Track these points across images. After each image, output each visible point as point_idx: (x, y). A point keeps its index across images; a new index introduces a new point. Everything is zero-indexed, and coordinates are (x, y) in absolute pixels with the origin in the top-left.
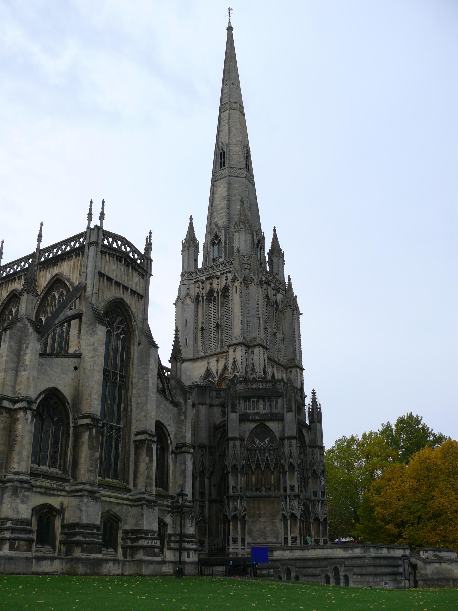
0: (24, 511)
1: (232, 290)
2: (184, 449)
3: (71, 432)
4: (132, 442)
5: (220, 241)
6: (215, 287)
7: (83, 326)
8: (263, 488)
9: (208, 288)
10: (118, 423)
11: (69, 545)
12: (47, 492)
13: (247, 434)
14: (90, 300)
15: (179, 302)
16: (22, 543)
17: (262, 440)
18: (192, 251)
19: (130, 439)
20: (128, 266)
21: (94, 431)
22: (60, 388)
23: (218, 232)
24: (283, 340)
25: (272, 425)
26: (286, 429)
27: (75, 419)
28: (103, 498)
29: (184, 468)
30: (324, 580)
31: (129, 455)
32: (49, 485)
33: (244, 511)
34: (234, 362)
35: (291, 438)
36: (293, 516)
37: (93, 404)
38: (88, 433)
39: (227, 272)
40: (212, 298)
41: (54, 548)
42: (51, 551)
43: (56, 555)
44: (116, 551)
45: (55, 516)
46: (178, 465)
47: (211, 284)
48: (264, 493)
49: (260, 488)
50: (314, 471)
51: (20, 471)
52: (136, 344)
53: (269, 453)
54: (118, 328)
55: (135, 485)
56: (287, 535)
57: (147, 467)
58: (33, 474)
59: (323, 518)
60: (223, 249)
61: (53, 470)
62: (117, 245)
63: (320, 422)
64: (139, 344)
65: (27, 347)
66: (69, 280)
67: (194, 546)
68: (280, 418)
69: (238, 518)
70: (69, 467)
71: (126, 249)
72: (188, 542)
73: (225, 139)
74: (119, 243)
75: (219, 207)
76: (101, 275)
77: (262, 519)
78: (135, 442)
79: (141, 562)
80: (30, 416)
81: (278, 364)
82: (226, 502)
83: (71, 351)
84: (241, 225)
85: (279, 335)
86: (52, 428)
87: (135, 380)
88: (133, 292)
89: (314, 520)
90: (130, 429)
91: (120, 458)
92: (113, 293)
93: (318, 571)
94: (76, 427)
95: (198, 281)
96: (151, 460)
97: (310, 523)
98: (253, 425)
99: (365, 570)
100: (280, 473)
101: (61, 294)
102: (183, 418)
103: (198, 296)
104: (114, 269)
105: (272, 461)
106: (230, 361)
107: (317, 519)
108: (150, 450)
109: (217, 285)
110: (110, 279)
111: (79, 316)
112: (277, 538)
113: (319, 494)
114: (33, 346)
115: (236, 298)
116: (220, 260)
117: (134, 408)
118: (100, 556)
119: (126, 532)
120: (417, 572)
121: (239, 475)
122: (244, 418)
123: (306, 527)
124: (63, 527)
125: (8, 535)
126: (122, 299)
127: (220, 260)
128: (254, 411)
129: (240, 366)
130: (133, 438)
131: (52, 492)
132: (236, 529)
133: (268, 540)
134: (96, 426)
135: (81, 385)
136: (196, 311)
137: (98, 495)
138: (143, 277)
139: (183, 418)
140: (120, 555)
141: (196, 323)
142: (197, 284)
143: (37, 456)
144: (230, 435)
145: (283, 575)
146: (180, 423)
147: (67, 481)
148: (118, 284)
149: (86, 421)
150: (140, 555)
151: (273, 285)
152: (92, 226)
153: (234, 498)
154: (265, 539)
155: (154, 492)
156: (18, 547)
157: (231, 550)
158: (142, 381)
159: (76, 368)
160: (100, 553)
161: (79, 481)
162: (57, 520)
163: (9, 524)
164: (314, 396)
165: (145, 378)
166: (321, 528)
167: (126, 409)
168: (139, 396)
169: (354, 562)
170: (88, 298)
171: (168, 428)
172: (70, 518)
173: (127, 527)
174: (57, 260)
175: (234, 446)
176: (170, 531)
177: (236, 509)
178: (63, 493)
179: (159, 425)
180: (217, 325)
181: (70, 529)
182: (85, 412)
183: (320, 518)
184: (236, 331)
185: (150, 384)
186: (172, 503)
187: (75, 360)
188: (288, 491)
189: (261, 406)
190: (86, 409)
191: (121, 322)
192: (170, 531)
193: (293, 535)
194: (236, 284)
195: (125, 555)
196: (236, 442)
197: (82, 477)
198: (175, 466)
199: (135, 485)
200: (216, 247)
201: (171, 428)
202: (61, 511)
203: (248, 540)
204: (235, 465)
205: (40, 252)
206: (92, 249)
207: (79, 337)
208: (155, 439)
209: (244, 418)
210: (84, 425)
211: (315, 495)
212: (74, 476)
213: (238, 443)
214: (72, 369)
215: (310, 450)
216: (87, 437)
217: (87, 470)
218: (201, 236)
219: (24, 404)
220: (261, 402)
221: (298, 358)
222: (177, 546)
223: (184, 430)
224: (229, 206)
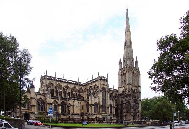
1: (126, 74)
6: (124, 73)
11: (99, 121)
12: (96, 115)
15: (119, 76)
18: (120, 64)
25: (129, 101)
36: (132, 115)
37: (101, 104)
57: (109, 110)
58: (95, 113)
73: (126, 39)
86: (96, 107)
94: (99, 107)
109: (125, 72)
114: (93, 97)
115: (127, 75)
122: (126, 100)
143: (95, 111)
146: (113, 103)
172: (99, 118)
176: (112, 118)
179: (110, 104)
181: (99, 119)
184: (127, 82)
192: (112, 118)
201: (112, 104)
209: (126, 100)
213: (125, 104)
217: (101, 112)
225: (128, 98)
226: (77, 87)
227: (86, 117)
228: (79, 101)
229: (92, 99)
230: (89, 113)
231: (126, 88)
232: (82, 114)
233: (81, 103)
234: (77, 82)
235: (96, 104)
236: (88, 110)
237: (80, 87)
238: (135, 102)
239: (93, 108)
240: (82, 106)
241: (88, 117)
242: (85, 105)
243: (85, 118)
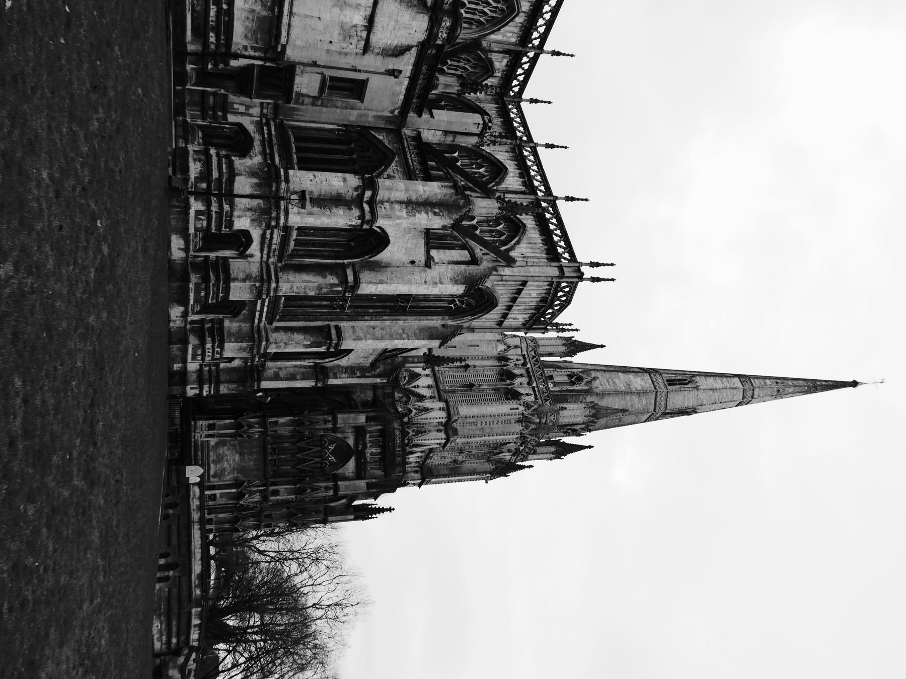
0: (242, 223)
2: (321, 376)
3: (338, 261)
4: (327, 323)
5: (573, 383)
6: (518, 381)
7: (463, 267)
9: (516, 372)
10: (350, 307)
13: (340, 435)
14: (494, 273)
16: (205, 223)
17: (333, 453)
19: (331, 321)
20: (536, 309)
21: (340, 289)
22: (389, 248)
23: (585, 381)
24: (455, 461)
25: (351, 465)
26: (347, 483)
27: (353, 264)
28: (259, 302)
29: (298, 377)
30: (163, 551)
31: (313, 321)
32: (274, 241)
33: (248, 436)
34: (427, 410)
35: (336, 488)
36: (240, 496)
38: (336, 282)
39: (536, 395)
40: (504, 377)
41: (200, 250)
42: (196, 246)
43: (191, 253)
44: (197, 313)
45: (237, 250)
46: (301, 370)
47: (521, 376)
50: (296, 514)
51: (290, 216)
52: (443, 322)
53: (318, 463)
54: (462, 302)
55: (277, 329)
56: (219, 489)
58: (287, 229)
60: (565, 388)
61: (292, 244)
62: (561, 296)
63: (355, 519)
64: (443, 325)
65: (435, 214)
66: (518, 243)
67: (205, 394)
68: (359, 475)
70: (296, 261)
71: (557, 305)
72: (210, 388)
74: (563, 299)
75: (617, 381)
76: (524, 283)
77: (237, 457)
78: (328, 326)
79: (186, 342)
80: (354, 223)
81: (427, 457)
82: (258, 414)
83: (433, 253)
84: (594, 411)
85: (461, 457)
87: (401, 323)
88: (505, 316)
90: (343, 320)
91: (309, 310)
92: (503, 295)
93: (174, 541)
94: (344, 267)
95: (525, 359)
96: (306, 346)
98: (351, 442)
99: (174, 603)
100: (293, 477)
101: (501, 234)
102: (358, 374)
103: (506, 359)
104: (532, 294)
105: (308, 466)
106: (427, 404)
108: (319, 345)
109: (520, 384)
110: (519, 292)
111: (474, 261)
112: (215, 476)
115: (504, 408)
116: (550, 385)
117: (368, 323)
118: (192, 302)
119: (221, 322)
120: (171, 656)
121: (291, 428)
122: (360, 432)
124: (226, 259)
125: (214, 208)
126: (497, 306)
127: (550, 385)
129: (423, 417)
130: (333, 324)
131: (267, 241)
132: (226, 427)
133: (212, 466)
134: (345, 291)
135: (393, 269)
136: (489, 358)
137: (264, 296)
138: (524, 325)
139: (358, 374)
140: (192, 317)
141: (474, 358)
142: (521, 358)
144: (340, 416)
145: (170, 499)
147: (280, 259)
148: (514, 300)
149: (351, 278)
150: (193, 341)
151: (521, 448)
152: (583, 269)
153: (263, 424)
154: (213, 461)
155: (268, 351)
156: (200, 219)
157: (200, 423)
158: (400, 331)
159: (413, 262)
160: (195, 302)
161: (280, 274)
162: (233, 252)
163: (226, 207)
164: (387, 510)
165: (404, 336)
166: (227, 526)
167: (368, 314)
168: (382, 329)
169: (184, 587)
170: (497, 271)
171: (346, 358)
172: (238, 266)
173: (227, 323)
174: (542, 224)
175: (326, 422)
177: (250, 426)
178: (265, 256)
180: (471, 386)
182: (361, 276)
185: (396, 342)
186: (257, 366)
187: (423, 261)
188: (272, 488)
189: (374, 450)
190: (365, 276)
191: (468, 304)
193: (218, 495)
194: (521, 408)
195: (193, 322)
197: (285, 277)
198: (301, 367)
199: (277, 329)
200: (566, 379)
201: (344, 362)
202: (243, 255)
203: (213, 441)
204: (303, 424)
205: (553, 202)
206: (555, 272)
207: (450, 263)
208: (332, 350)
209: (360, 432)
210: (346, 277)
211: (269, 516)
212: (287, 268)
213: (330, 425)
214: (411, 259)
215: (322, 508)
216: (332, 281)
217: (293, 284)
218: (581, 358)
219: (368, 217)
221: (433, 480)
222: (206, 375)
223: (343, 375)
224: (617, 393)
225: (371, 451)
226: (509, 34)
227: (246, 113)
228: (406, 65)
229: (426, 205)
230: (288, 166)
231: (425, 392)
232: (275, 76)
233: (394, 73)
234: (544, 37)
235: (368, 242)
236: (320, 152)
237: (500, 63)
239: (342, 219)
240: (356, 89)
241: (240, 143)
242: (370, 119)
243: (237, 101)
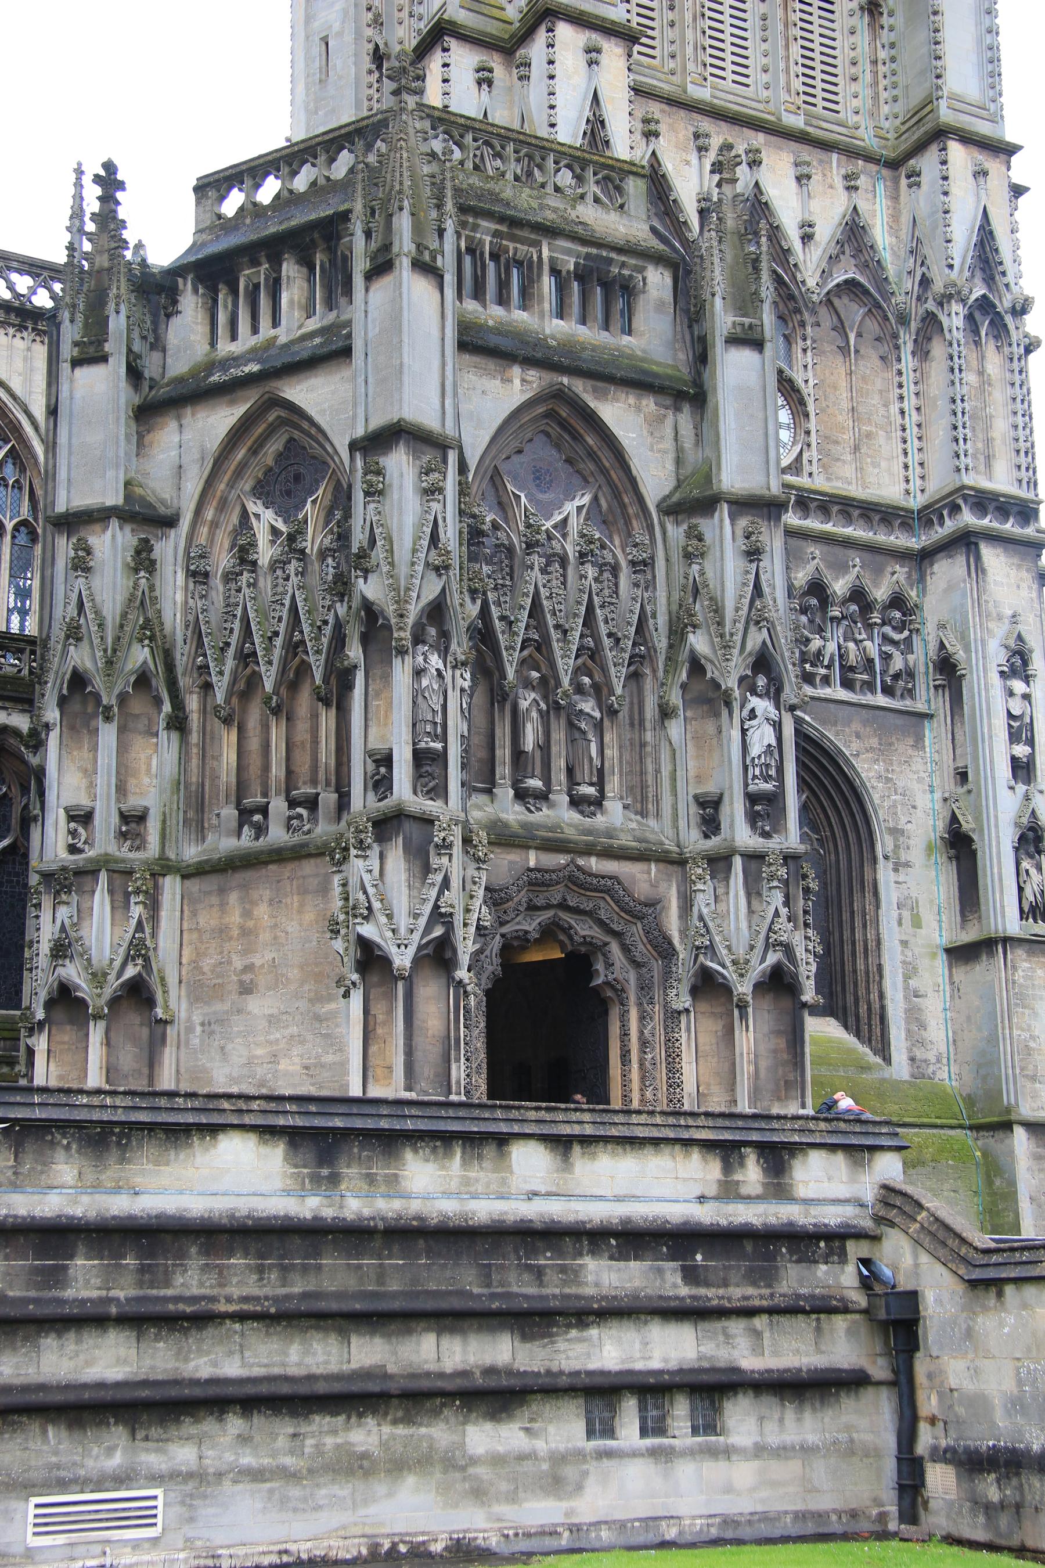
8: (278, 805)
48: (277, 834)
49: (264, 810)
50: (697, 666)
59: (758, 969)
69: (82, 1003)
89: (695, 992)
97: (673, 1016)
98: (218, 421)
107: (708, 985)
113: (735, 814)
123: (644, 1043)
128: (253, 341)
183: (730, 974)
196: (93, 541)
213: (111, 545)
215: (676, 532)
220: (289, 268)
238: (563, 430)
